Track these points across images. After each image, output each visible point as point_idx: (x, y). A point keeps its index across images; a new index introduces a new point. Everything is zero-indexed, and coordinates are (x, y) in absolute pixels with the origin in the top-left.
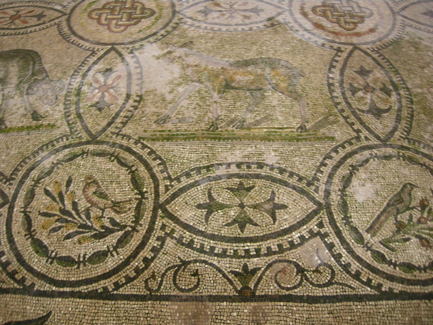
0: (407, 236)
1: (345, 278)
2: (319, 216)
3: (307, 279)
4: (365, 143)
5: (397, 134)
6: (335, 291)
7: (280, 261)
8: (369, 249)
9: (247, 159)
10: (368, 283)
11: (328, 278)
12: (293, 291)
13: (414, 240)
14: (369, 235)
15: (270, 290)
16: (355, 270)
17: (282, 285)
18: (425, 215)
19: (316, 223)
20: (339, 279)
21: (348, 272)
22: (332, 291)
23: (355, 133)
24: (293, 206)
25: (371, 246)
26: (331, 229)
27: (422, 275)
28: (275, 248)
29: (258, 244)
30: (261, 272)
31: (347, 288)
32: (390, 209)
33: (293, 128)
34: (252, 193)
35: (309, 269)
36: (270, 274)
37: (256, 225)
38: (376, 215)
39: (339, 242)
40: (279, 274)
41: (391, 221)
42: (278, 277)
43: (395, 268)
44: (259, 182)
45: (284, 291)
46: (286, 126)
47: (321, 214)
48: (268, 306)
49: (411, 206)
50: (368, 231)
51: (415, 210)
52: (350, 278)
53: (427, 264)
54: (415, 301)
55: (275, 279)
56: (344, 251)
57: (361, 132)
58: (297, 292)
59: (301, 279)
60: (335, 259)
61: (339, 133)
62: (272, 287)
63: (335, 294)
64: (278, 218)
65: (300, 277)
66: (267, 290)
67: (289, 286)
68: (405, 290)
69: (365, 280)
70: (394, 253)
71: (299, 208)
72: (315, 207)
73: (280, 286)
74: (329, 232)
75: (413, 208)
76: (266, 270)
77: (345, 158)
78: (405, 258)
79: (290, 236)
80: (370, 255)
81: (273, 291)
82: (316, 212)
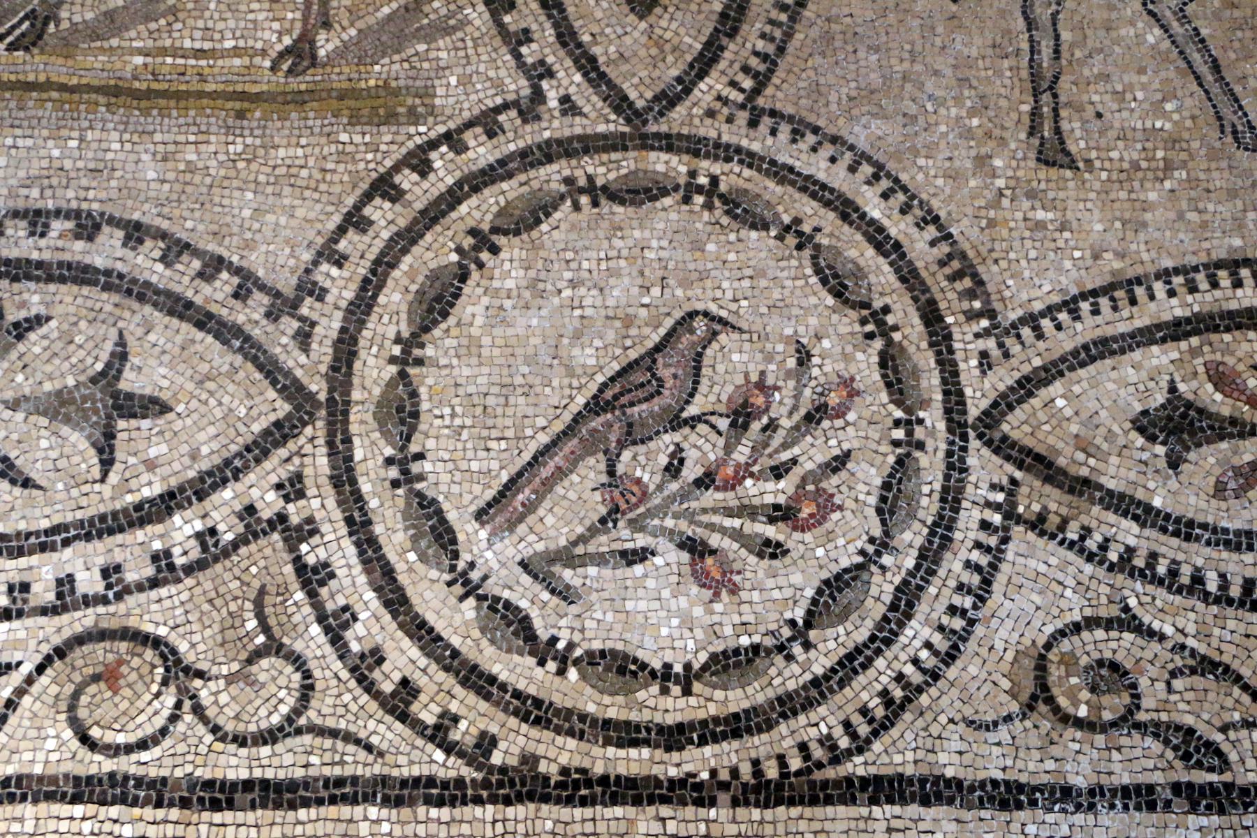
0: (641, 541)
1: (354, 707)
2: (292, 446)
3: (198, 710)
4: (553, 127)
5: (710, 87)
6: (302, 760)
7: (102, 635)
8: (471, 590)
9: (35, 193)
10: (438, 734)
11: (284, 709)
12: (134, 757)
13: (670, 556)
14: (483, 534)
15: (41, 756)
16: (397, 677)
17: (95, 733)
18: (742, 453)
19: (274, 479)
20: (325, 711)
21: (369, 687)
22: (288, 759)
23: (524, 82)
24: (194, 404)
25: (485, 578)
26: (331, 503)
27: (669, 702)
28: (89, 582)
29: (23, 562)
30: (16, 678)
31: (351, 748)
32: (596, 423)
33: (264, 53)
34: (35, 342)
35: (215, 670)
36: (54, 689)
37: (27, 483)
38: (533, 447)
39: (354, 560)
40: (92, 689)
41: (592, 470)
42: (84, 699)
43: (561, 672)
44: (67, 298)
45: (98, 757)
46: (229, 44)
47: (302, 440)
48: (21, 820)
49: (692, 410)
50: (481, 515)
51: (703, 428)
52: (373, 706)
53: (703, 657)
54: (618, 811)
55: (72, 708)
56: (370, 595)
57: (550, 74)
58: (150, 764)
59: (178, 705)
60: (327, 630)
61: (453, 80)
62: (51, 744)
63: (299, 773)
64: (119, 455)
65: (169, 700)
66: (27, 756)
67: (121, 739)
68: (586, 764)
69: (429, 718)
70: (574, 609)
71: (218, 413)
72: (284, 408)
73: (85, 739)
74: (318, 516)
75: (693, 422)
76: (40, 669)
77: (453, 198)
78: (614, 635)
79: (159, 528)
80: (471, 614)
81: (54, 757)
82: (280, 433)
